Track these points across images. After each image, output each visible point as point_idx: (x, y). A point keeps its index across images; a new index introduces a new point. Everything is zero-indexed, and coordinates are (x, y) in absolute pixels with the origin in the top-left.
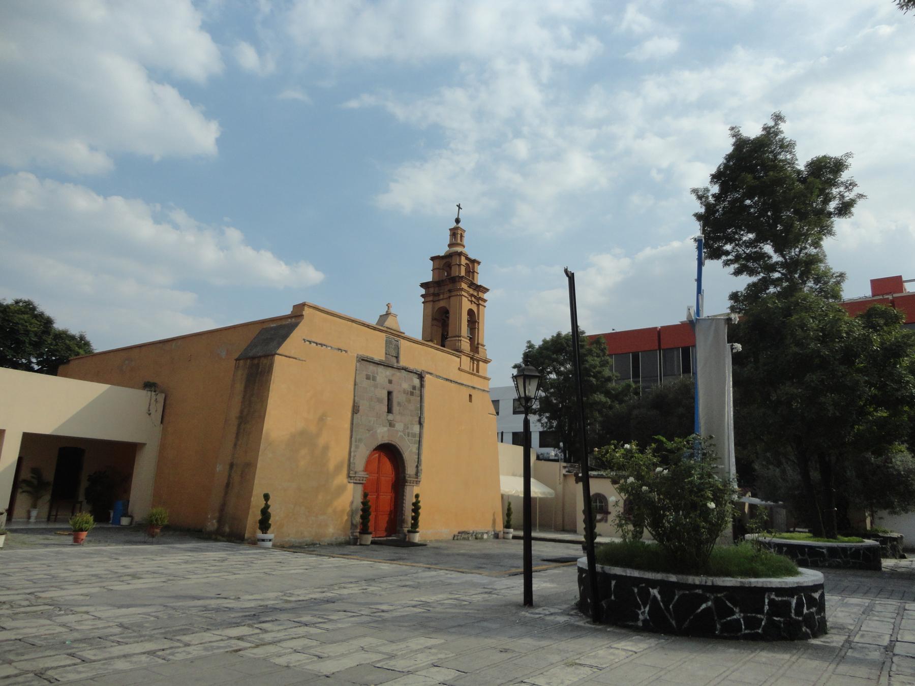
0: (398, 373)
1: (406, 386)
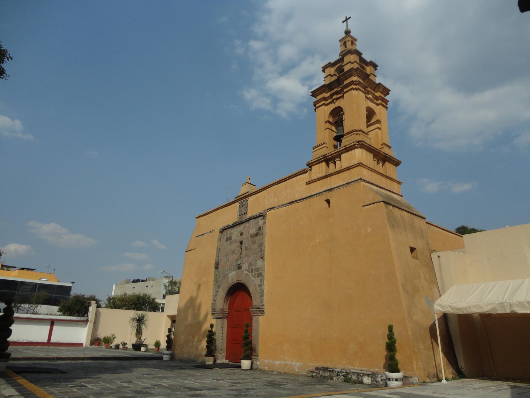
0: (247, 225)
1: (253, 231)
